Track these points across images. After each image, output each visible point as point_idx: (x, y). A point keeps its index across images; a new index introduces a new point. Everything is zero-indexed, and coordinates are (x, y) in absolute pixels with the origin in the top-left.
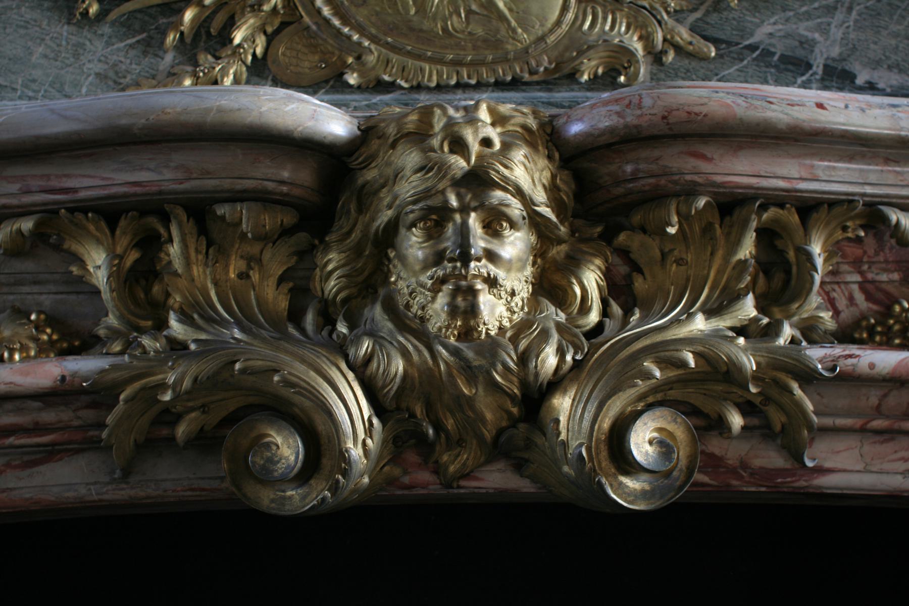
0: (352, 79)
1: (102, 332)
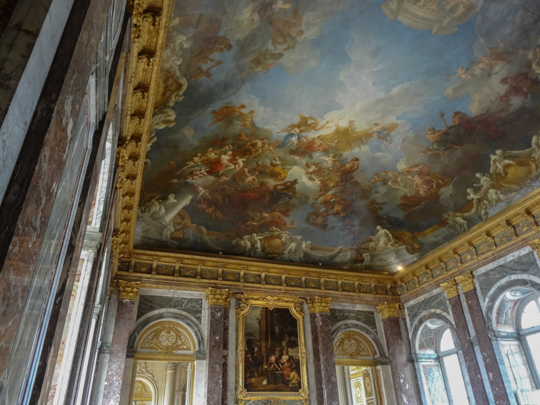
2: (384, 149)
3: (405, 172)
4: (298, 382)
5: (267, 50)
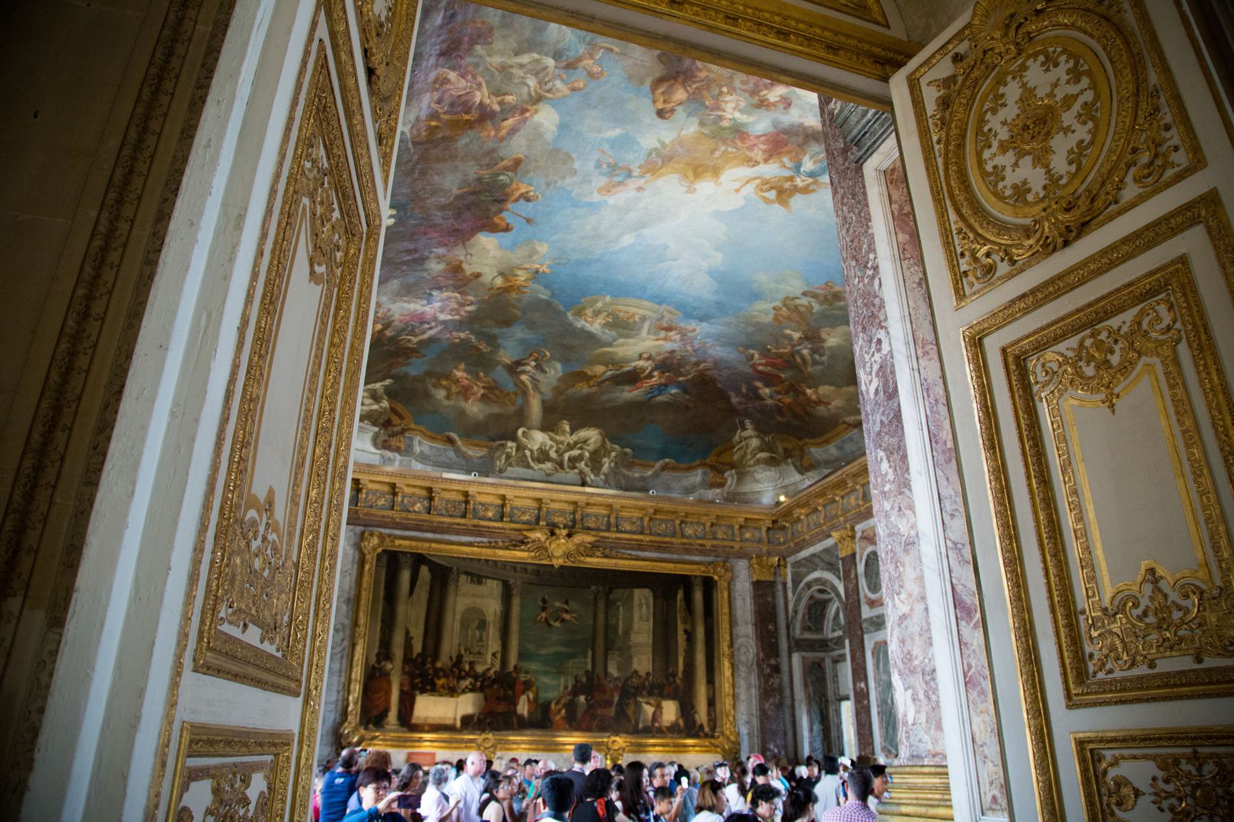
2: (606, 147)
3: (529, 107)
5: (821, 305)
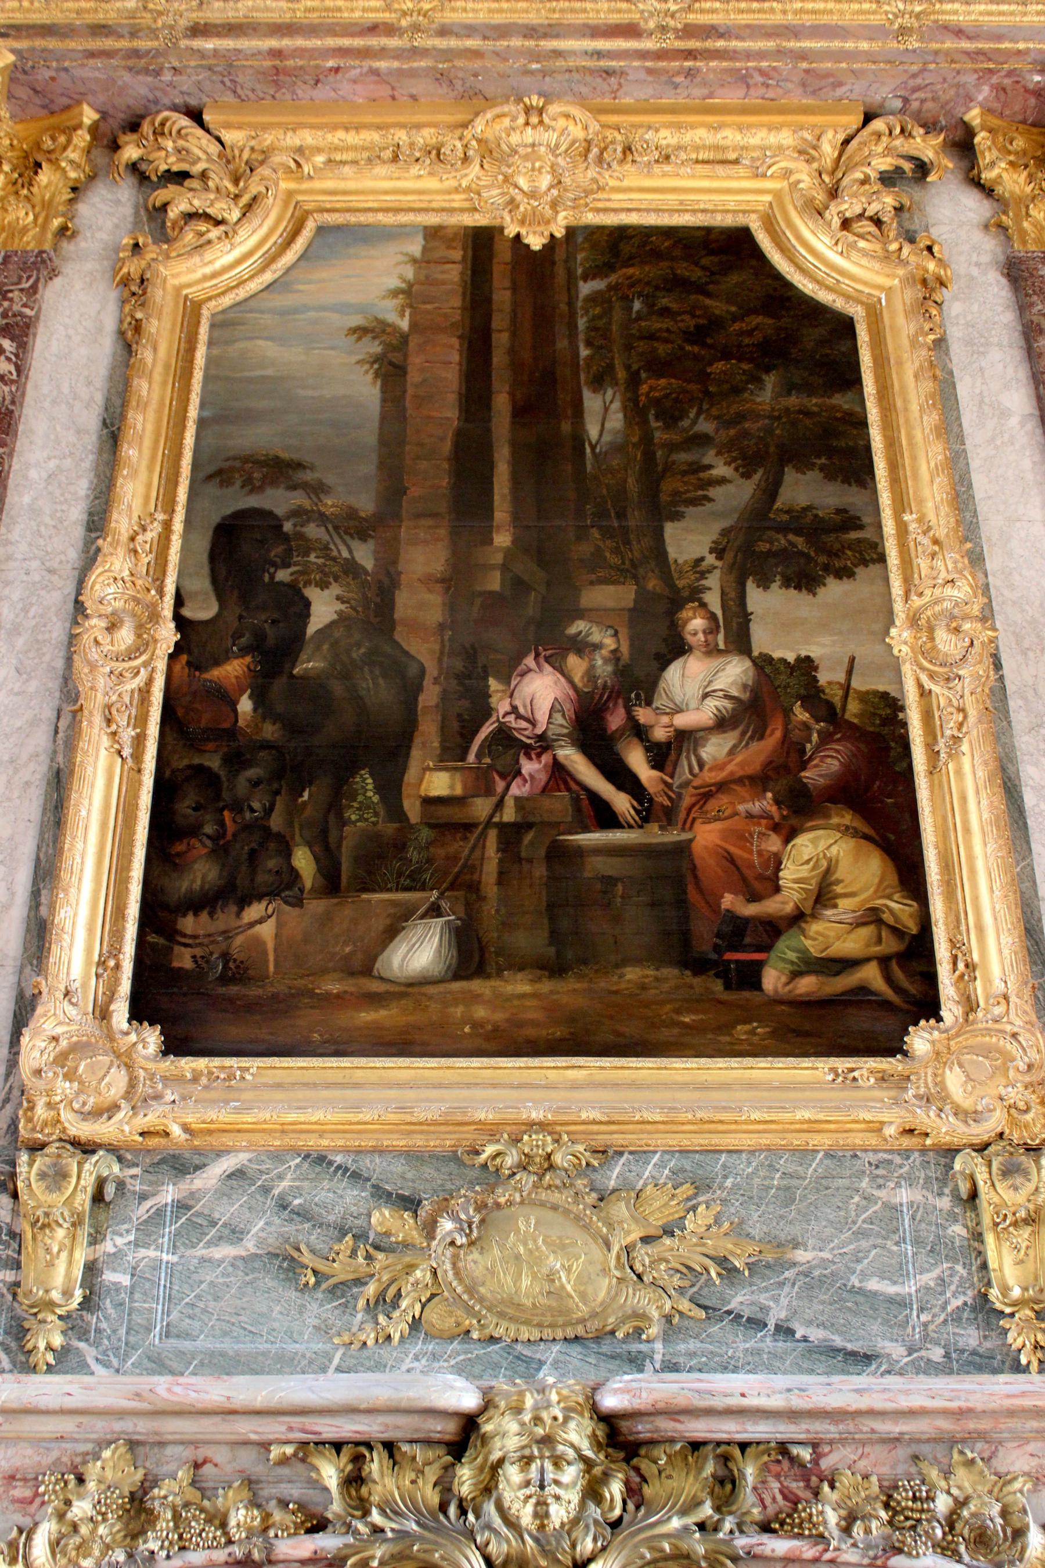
0: (475, 1335)
1: (330, 1516)
4: (890, 945)
